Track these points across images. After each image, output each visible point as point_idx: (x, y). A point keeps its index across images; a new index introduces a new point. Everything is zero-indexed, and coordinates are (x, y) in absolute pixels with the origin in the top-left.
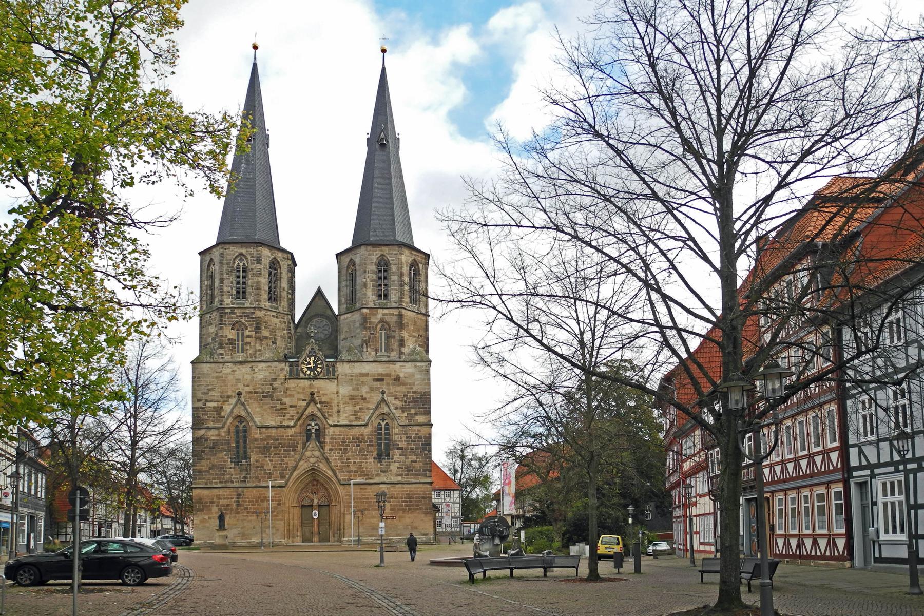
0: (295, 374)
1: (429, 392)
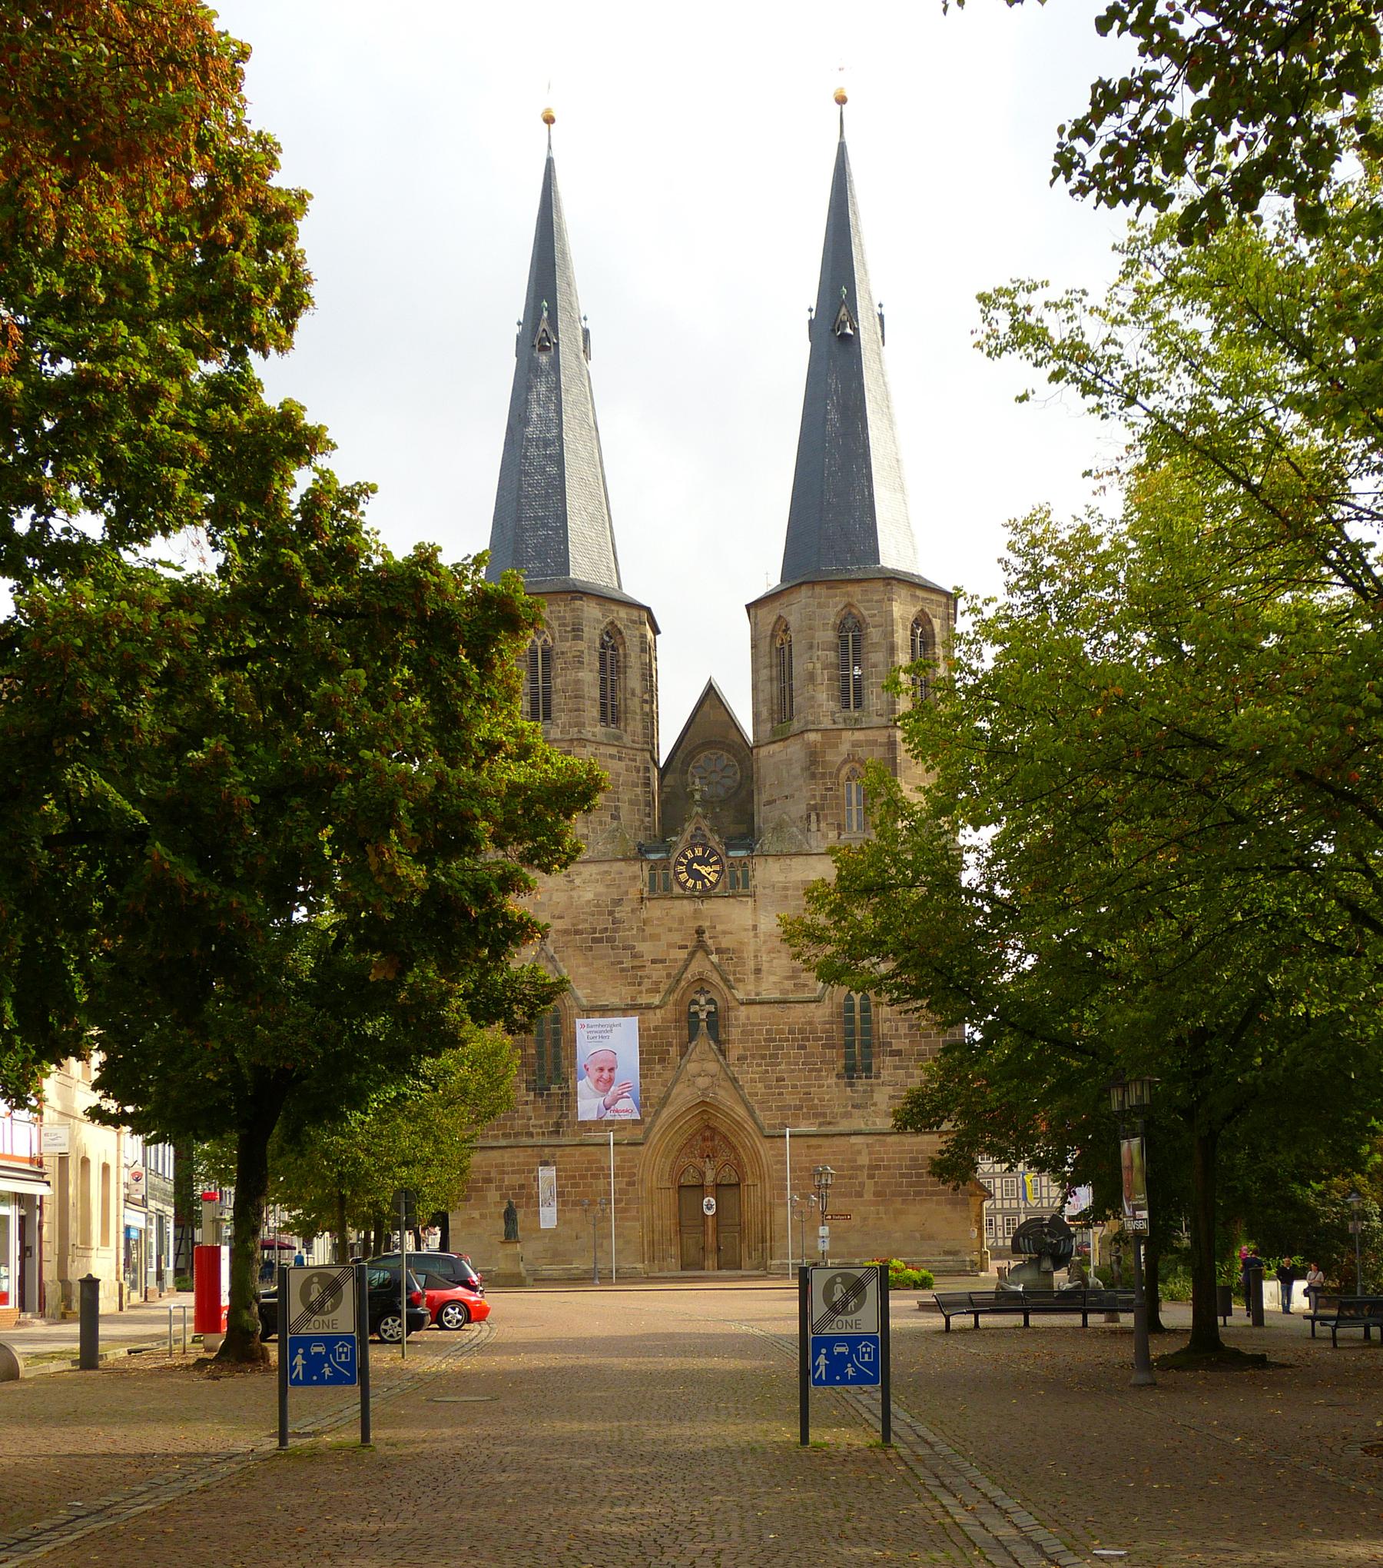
0: (660, 888)
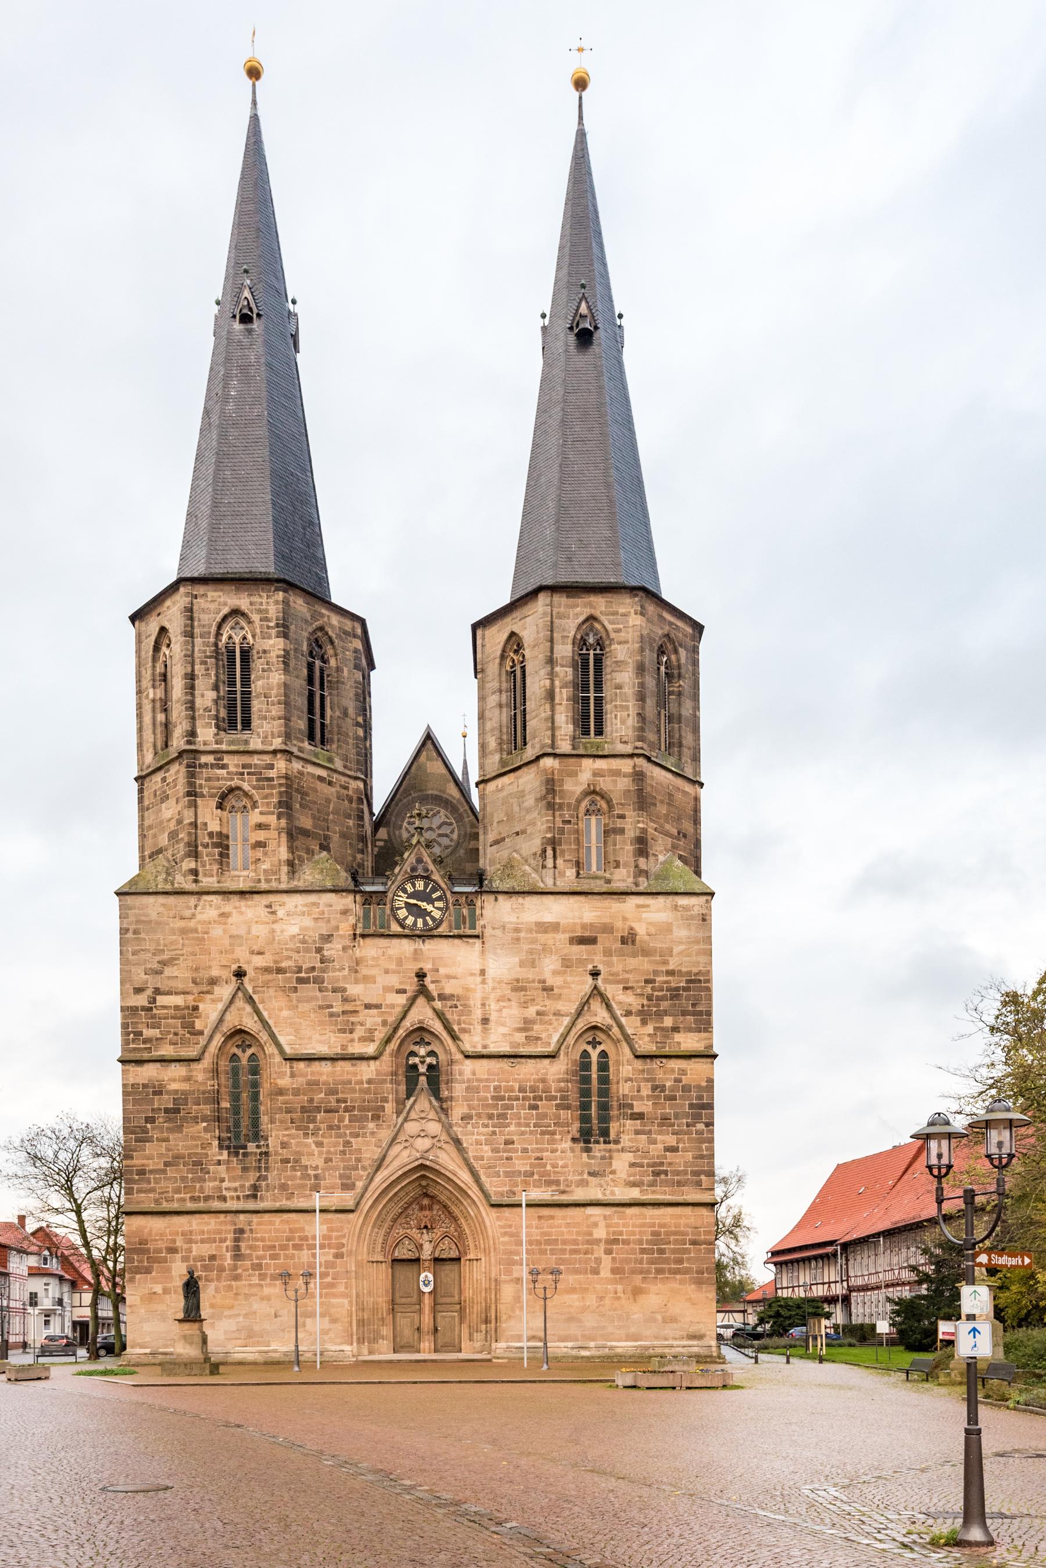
1: (709, 972)
